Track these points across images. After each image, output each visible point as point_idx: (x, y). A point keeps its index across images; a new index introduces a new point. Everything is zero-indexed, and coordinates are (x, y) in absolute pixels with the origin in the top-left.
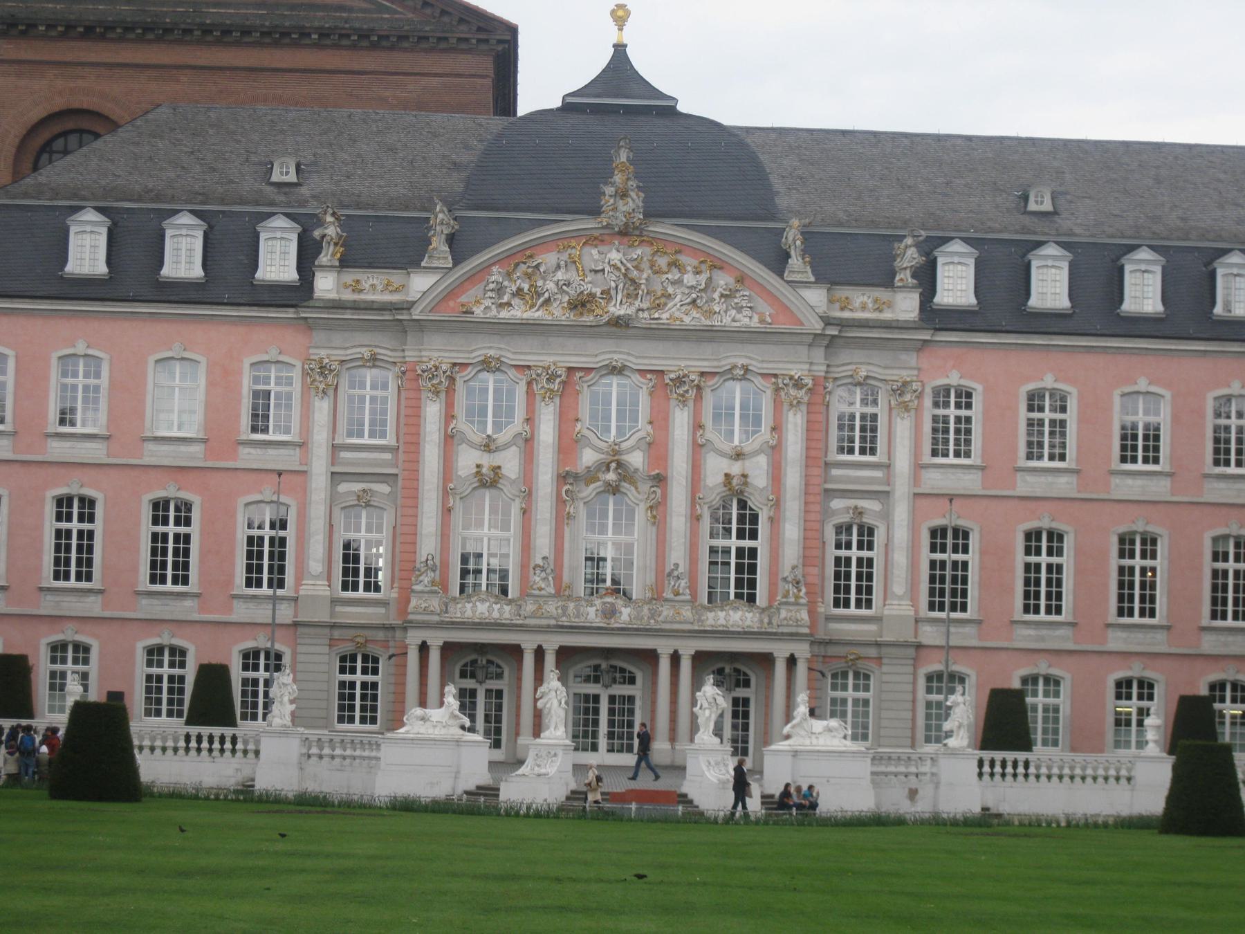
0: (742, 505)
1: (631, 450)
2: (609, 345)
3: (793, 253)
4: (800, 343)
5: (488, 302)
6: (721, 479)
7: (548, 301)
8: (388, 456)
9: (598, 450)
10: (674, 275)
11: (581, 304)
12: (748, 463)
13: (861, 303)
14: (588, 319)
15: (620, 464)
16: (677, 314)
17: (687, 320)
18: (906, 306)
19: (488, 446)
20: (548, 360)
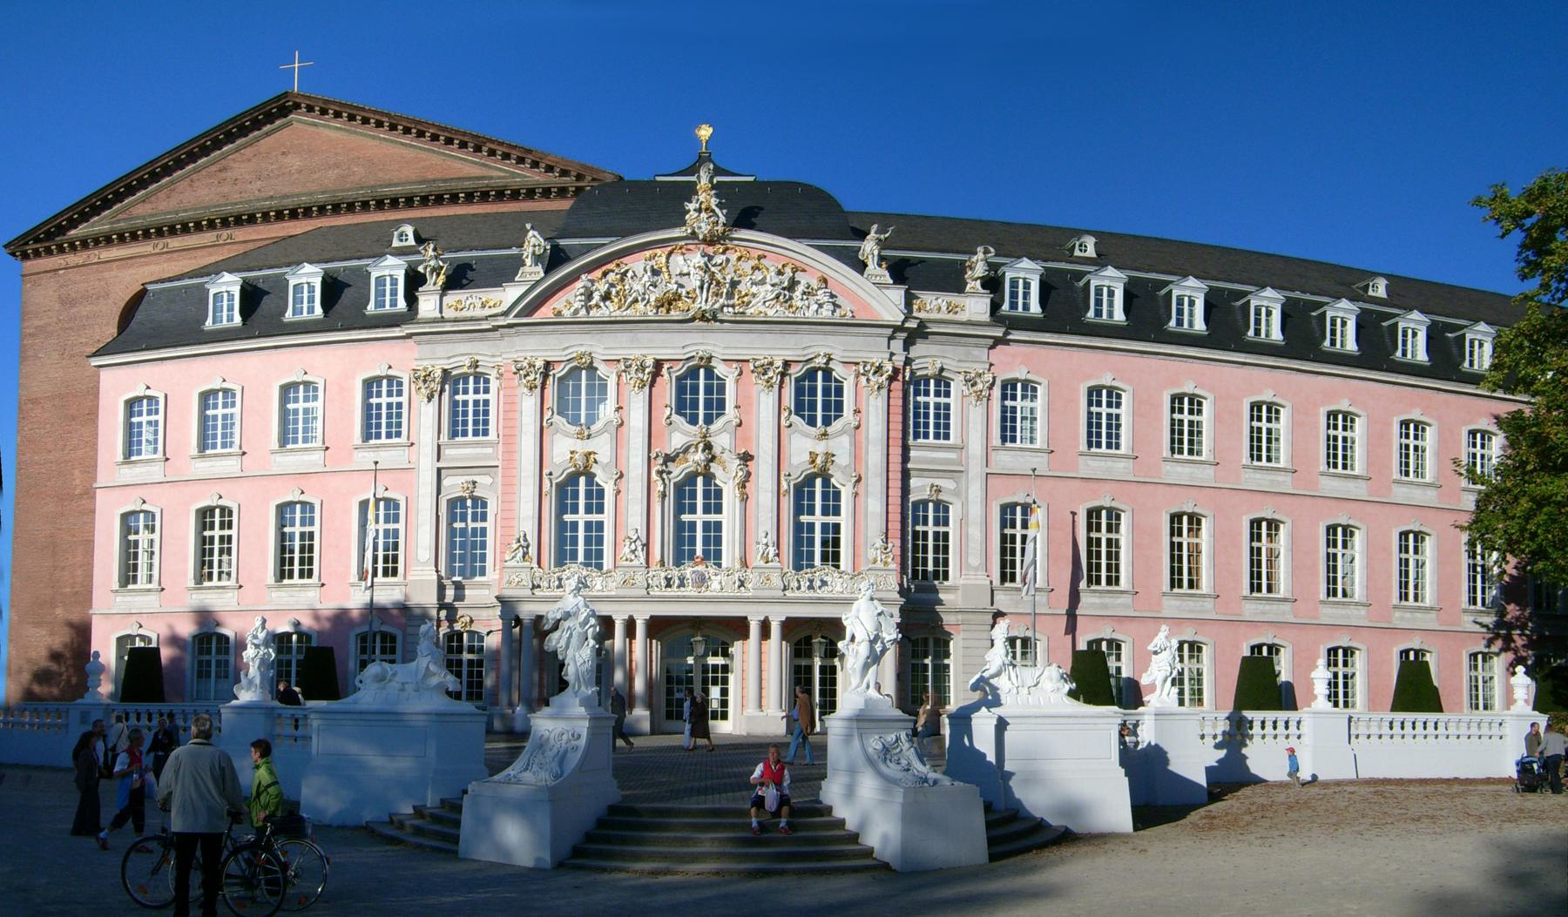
0: (826, 483)
1: (720, 431)
2: (696, 337)
3: (870, 262)
4: (879, 335)
5: (577, 305)
6: (807, 457)
7: (636, 301)
8: (490, 450)
9: (686, 433)
10: (758, 276)
11: (668, 302)
12: (831, 442)
13: (933, 304)
14: (675, 314)
15: (708, 447)
16: (762, 309)
17: (771, 312)
18: (975, 306)
19: (580, 436)
20: (635, 353)
